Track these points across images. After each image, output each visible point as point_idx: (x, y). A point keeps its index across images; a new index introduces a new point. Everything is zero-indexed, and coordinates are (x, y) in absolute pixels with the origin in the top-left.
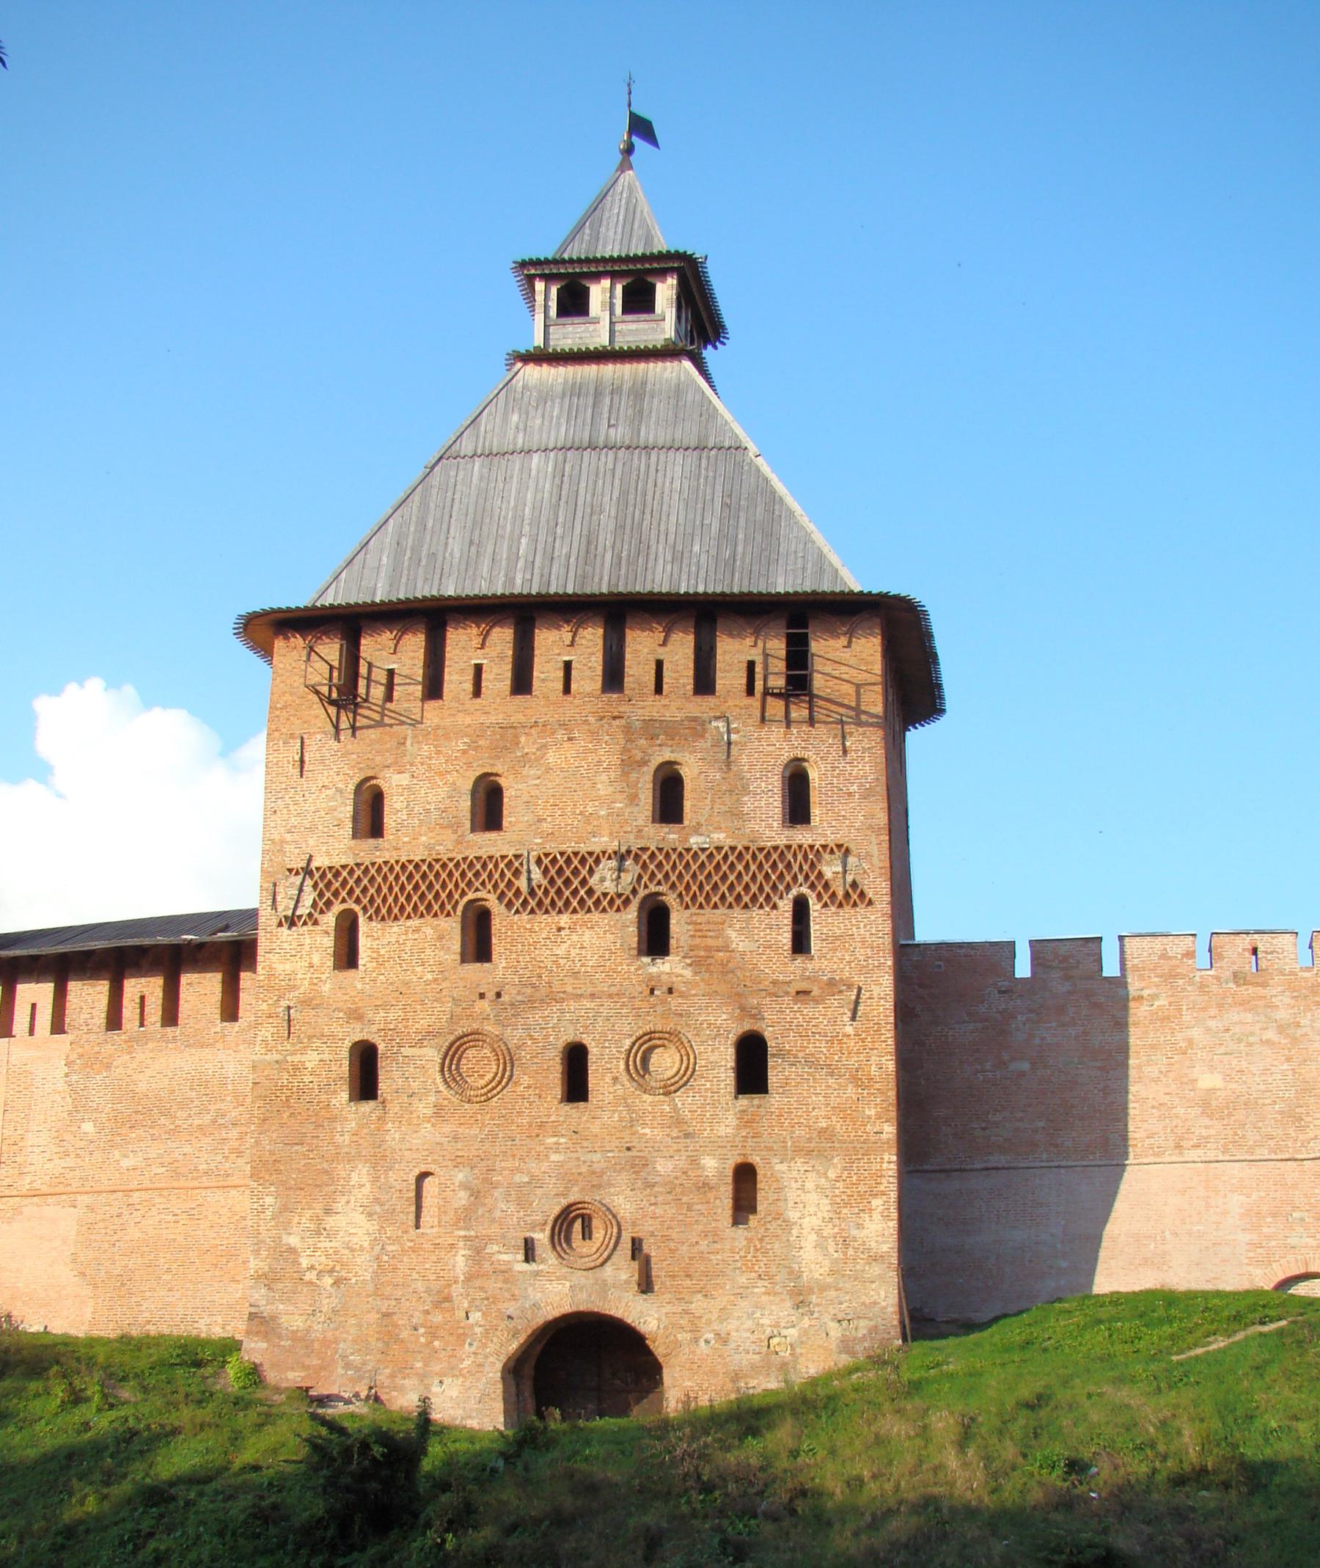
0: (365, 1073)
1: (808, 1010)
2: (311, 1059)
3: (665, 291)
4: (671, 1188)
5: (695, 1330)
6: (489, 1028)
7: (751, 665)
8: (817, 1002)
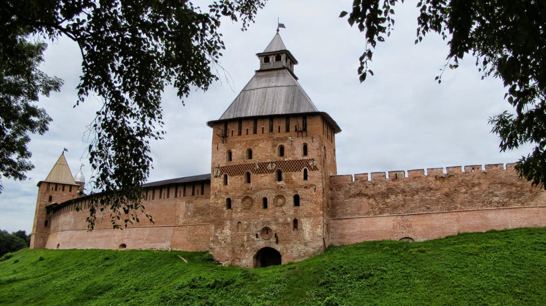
0: (229, 203)
1: (307, 190)
3: (283, 57)
4: (282, 224)
5: (287, 250)
6: (250, 195)
7: (296, 126)
8: (308, 189)
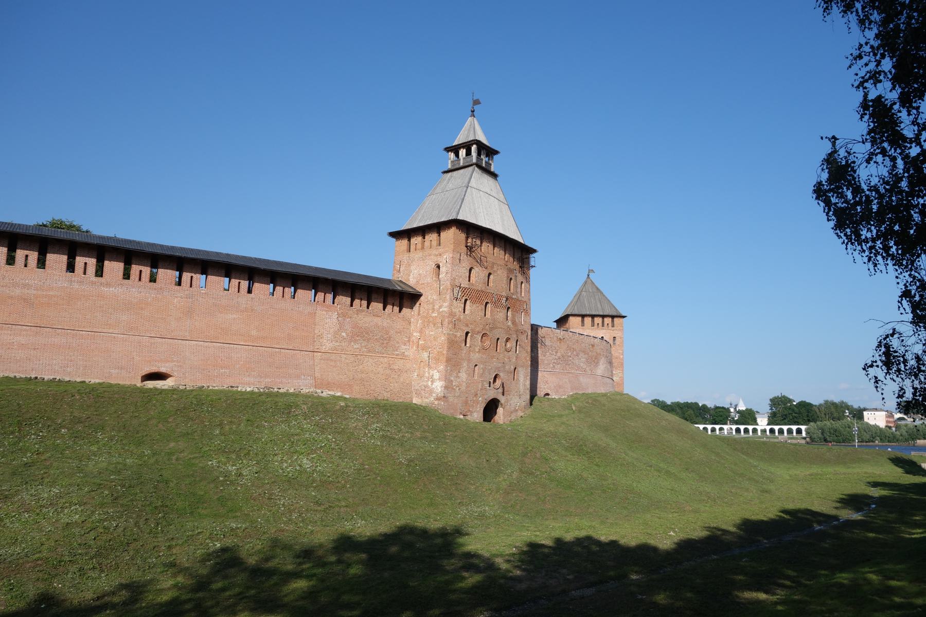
2: (458, 334)
